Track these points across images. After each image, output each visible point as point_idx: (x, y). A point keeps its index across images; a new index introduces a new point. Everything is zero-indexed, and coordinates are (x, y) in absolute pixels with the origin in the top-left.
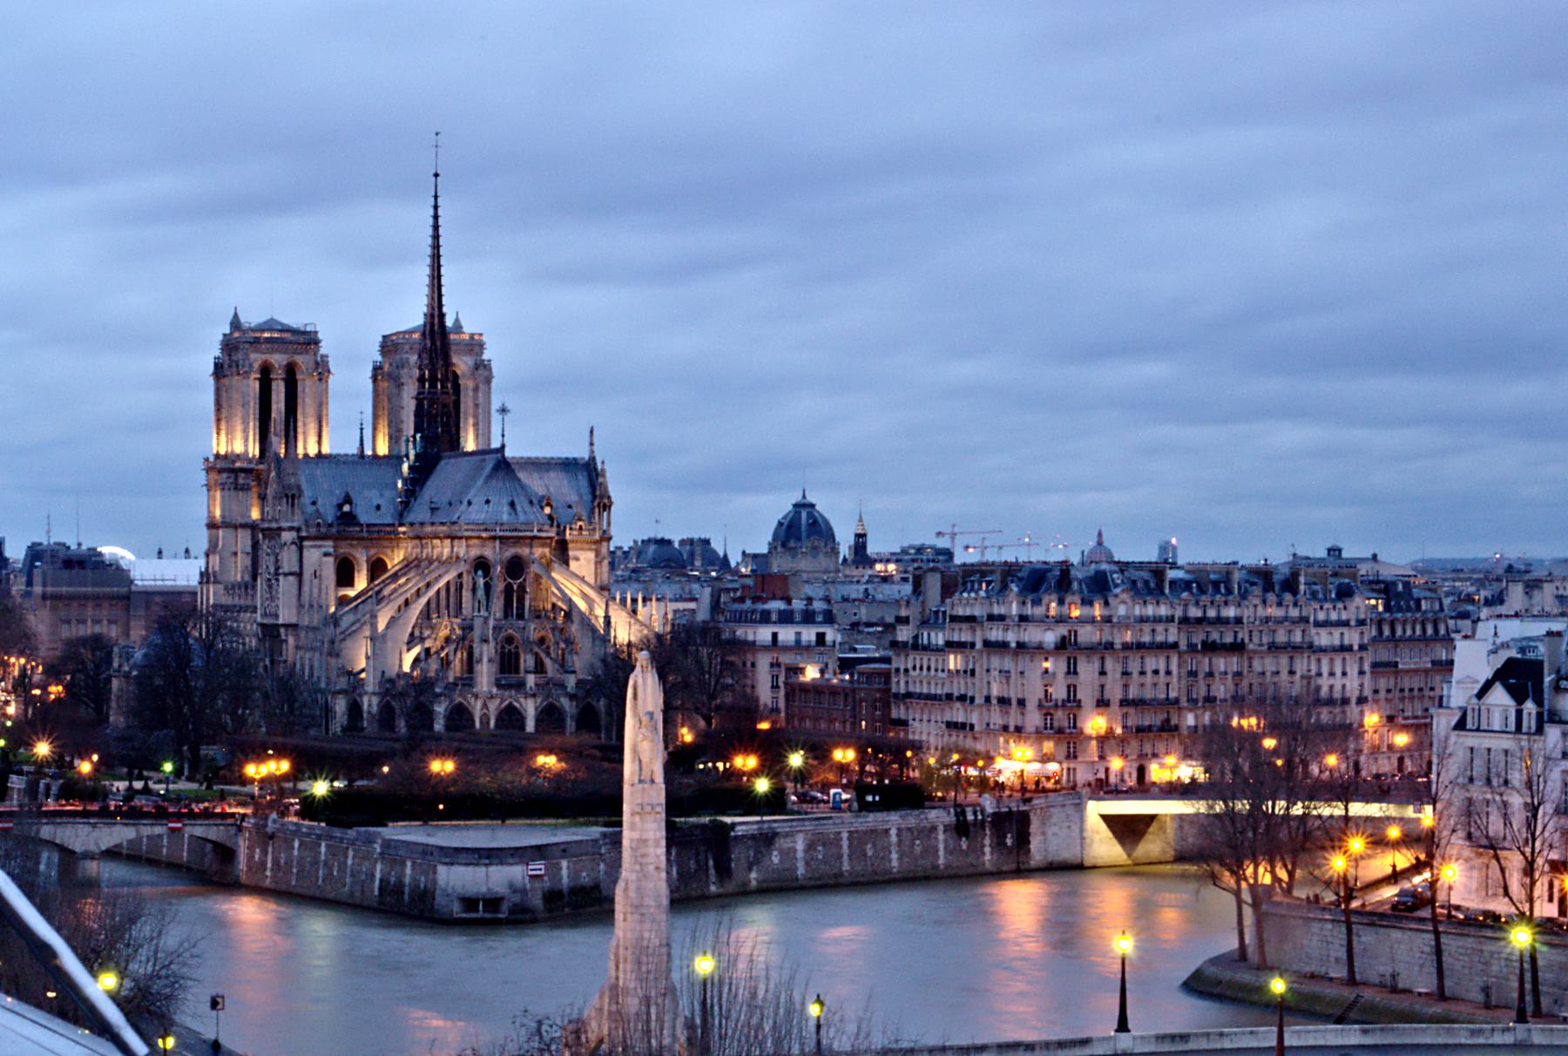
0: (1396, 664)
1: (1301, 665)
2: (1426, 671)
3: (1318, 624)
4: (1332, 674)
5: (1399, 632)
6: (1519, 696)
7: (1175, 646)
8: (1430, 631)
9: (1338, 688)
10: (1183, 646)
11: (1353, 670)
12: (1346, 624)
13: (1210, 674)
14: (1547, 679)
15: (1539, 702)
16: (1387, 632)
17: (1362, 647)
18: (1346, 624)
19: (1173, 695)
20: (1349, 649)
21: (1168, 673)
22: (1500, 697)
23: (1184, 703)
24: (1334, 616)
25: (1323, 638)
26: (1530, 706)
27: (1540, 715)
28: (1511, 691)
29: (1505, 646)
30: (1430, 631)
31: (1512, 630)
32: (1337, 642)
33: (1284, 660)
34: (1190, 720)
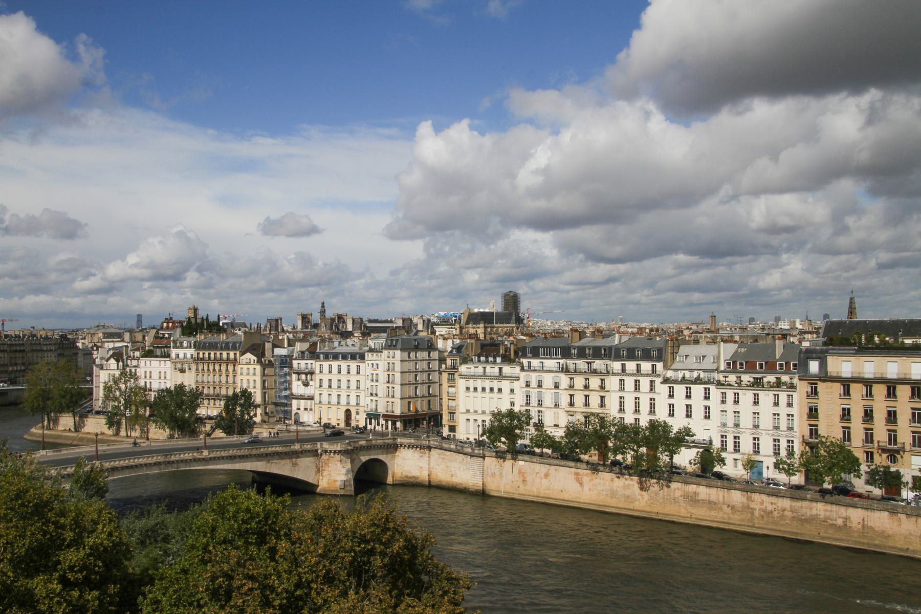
0: (63, 354)
1: (40, 354)
2: (71, 355)
3: (44, 345)
4: (48, 357)
5: (64, 346)
6: (118, 361)
7: (6, 351)
8: (72, 346)
9: (49, 361)
10: (8, 350)
11: (53, 356)
12: (51, 344)
13: (15, 358)
14: (125, 357)
15: (123, 363)
16: (61, 346)
17: (55, 350)
18: (51, 344)
19: (6, 362)
20: (52, 350)
21: (4, 357)
22: (112, 361)
23: (9, 364)
24: (48, 343)
25: (45, 348)
26: (121, 363)
27: (123, 365)
28: (115, 359)
29: (113, 349)
30: (72, 346)
31: (111, 345)
32: (48, 349)
33: (35, 354)
34: (11, 369)
